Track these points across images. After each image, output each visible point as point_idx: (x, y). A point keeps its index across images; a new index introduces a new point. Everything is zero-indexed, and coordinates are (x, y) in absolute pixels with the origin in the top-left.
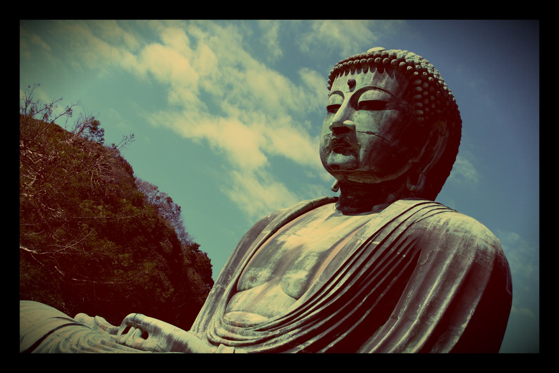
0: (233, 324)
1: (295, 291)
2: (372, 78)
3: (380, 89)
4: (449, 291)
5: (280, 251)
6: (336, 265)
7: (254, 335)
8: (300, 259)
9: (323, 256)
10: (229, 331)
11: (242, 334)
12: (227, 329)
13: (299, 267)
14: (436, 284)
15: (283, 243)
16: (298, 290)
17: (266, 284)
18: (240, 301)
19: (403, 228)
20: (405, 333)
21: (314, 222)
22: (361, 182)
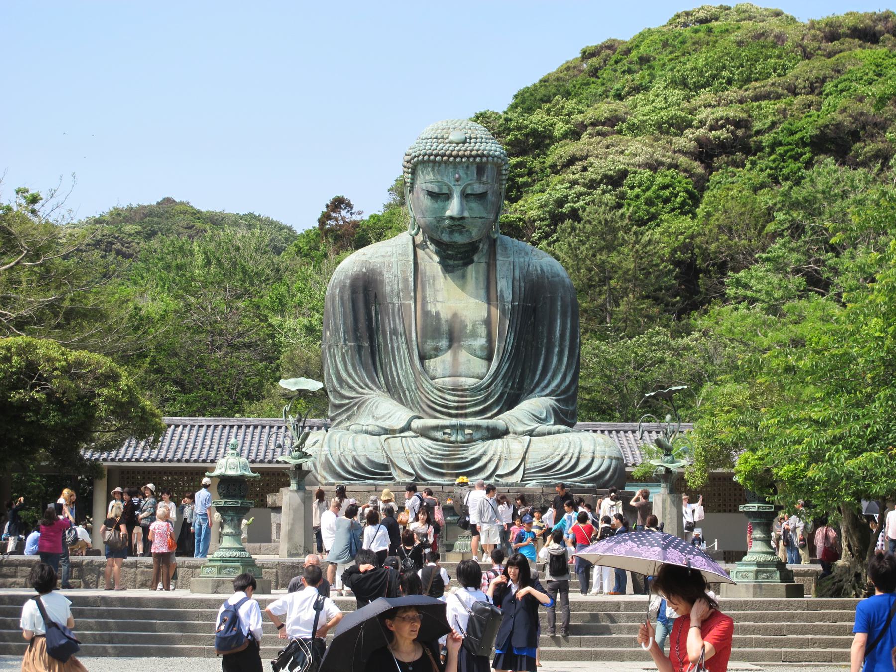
0: (453, 390)
1: (485, 354)
4: (567, 323)
5: (443, 321)
6: (504, 329)
7: (480, 395)
8: (469, 327)
9: (488, 322)
10: (459, 396)
11: (471, 396)
12: (455, 395)
13: (474, 335)
14: (558, 321)
15: (437, 313)
17: (450, 352)
19: (522, 284)
20: (552, 358)
21: (437, 282)
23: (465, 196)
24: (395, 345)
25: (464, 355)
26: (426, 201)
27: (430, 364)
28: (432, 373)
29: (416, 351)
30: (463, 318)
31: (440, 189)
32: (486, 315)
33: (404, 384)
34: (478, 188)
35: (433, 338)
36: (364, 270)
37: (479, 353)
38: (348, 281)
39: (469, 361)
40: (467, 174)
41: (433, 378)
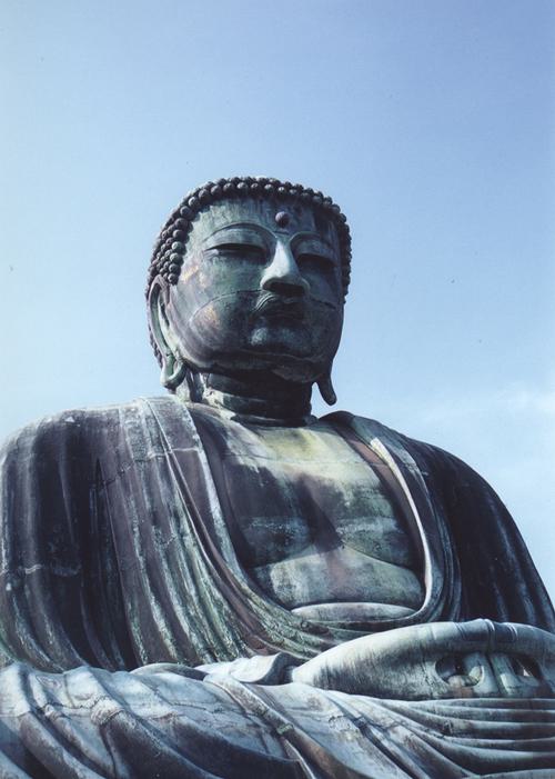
1: (401, 554)
2: (313, 225)
3: (329, 245)
8: (348, 498)
9: (387, 489)
13: (362, 510)
14: (503, 531)
15: (264, 472)
16: (402, 554)
18: (294, 583)
22: (287, 378)
23: (299, 258)
24: (159, 550)
25: (352, 557)
26: (219, 267)
27: (276, 573)
28: (283, 595)
29: (226, 542)
30: (326, 483)
31: (244, 236)
32: (376, 479)
33: (195, 639)
34: (318, 247)
35: (267, 514)
36: (70, 420)
37: (386, 548)
38: (30, 442)
39: (369, 565)
40: (298, 220)
41: (289, 605)
